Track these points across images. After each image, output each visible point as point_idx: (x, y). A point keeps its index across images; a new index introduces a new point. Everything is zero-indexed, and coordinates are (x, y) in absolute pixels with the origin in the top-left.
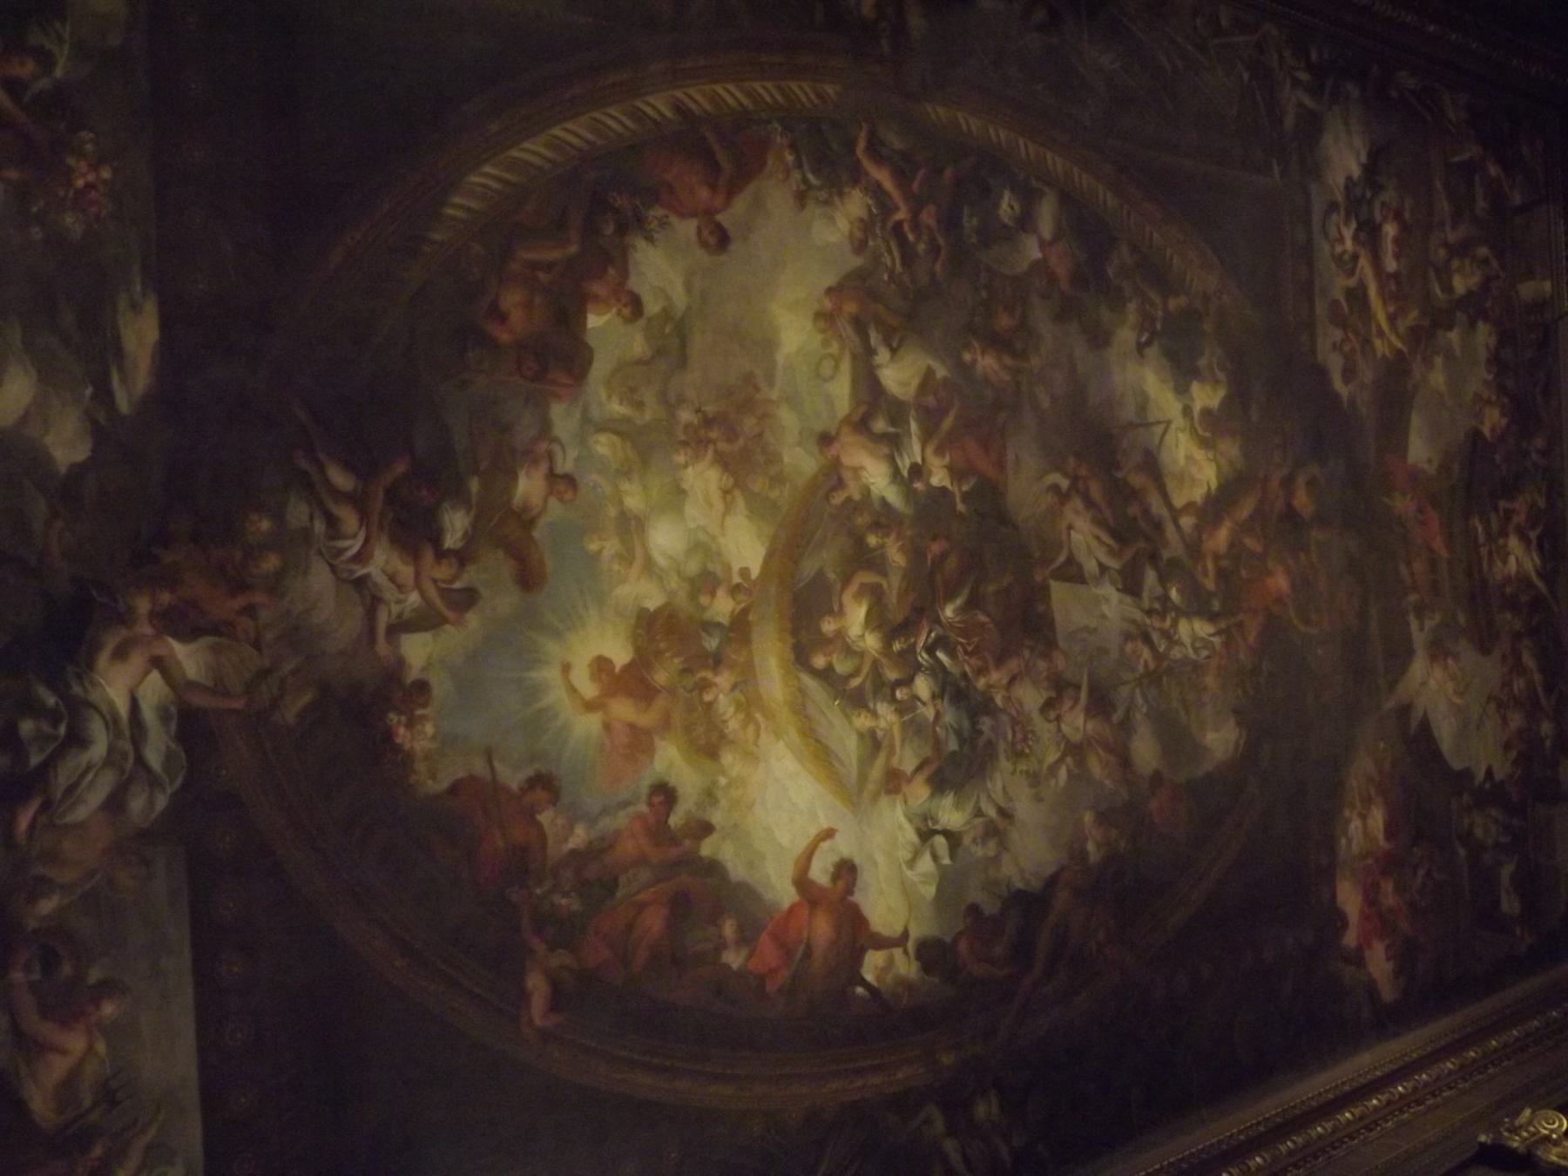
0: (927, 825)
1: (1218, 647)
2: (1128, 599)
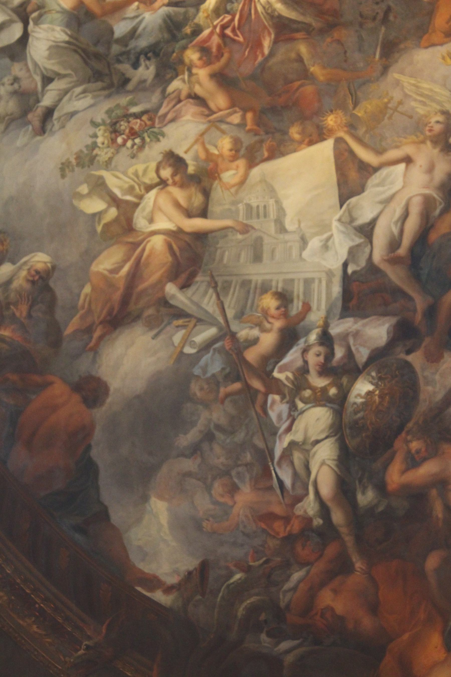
0: (34, 11)
1: (299, 509)
2: (337, 289)
